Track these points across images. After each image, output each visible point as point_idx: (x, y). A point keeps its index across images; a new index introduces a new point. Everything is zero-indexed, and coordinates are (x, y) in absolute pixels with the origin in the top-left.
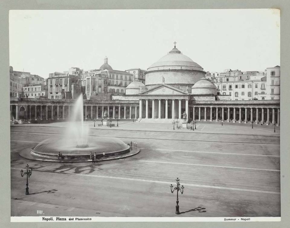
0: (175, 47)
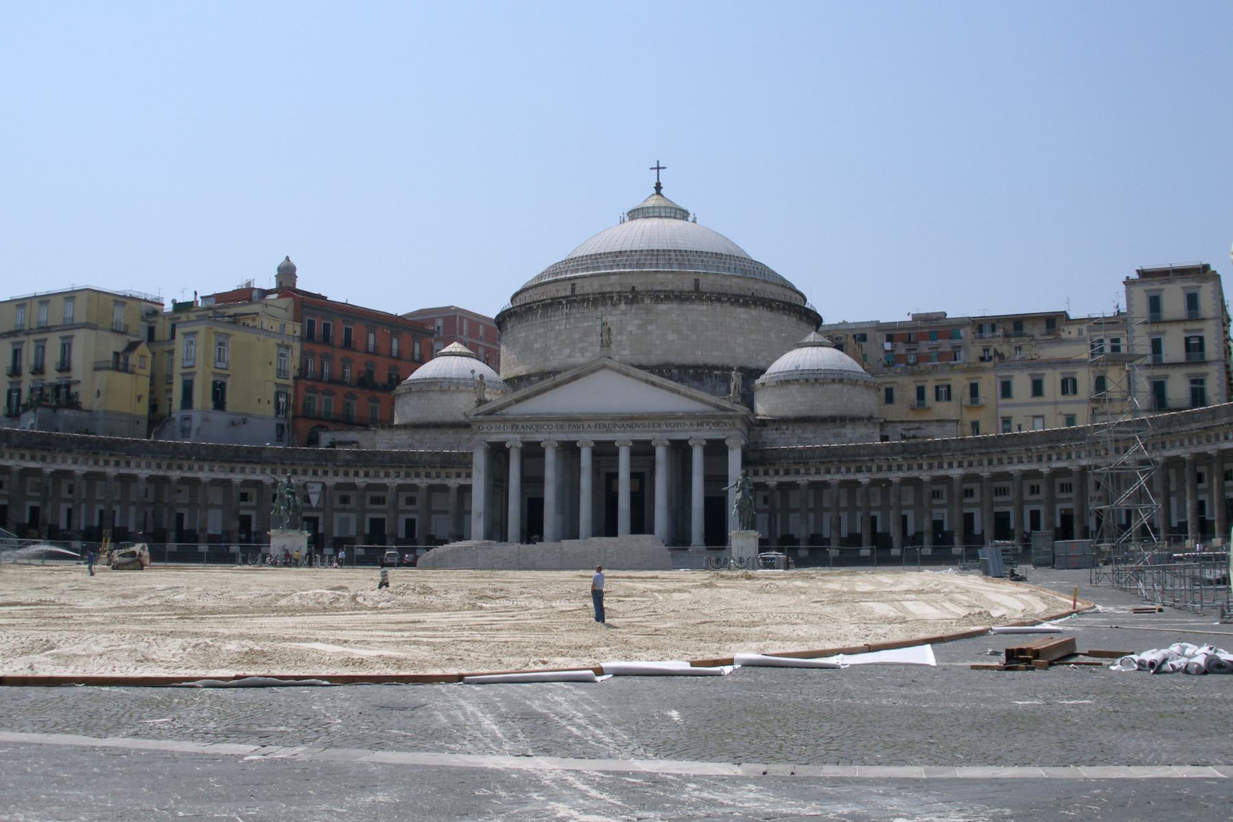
0: (658, 187)
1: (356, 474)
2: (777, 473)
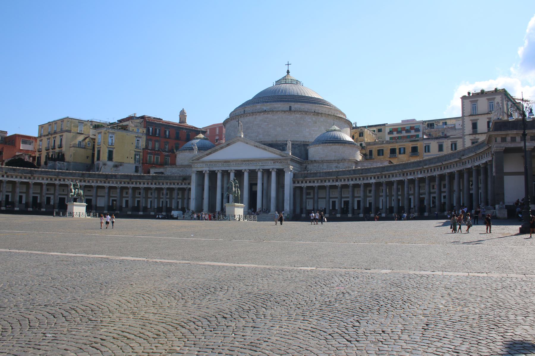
1: (152, 184)
2: (306, 182)
